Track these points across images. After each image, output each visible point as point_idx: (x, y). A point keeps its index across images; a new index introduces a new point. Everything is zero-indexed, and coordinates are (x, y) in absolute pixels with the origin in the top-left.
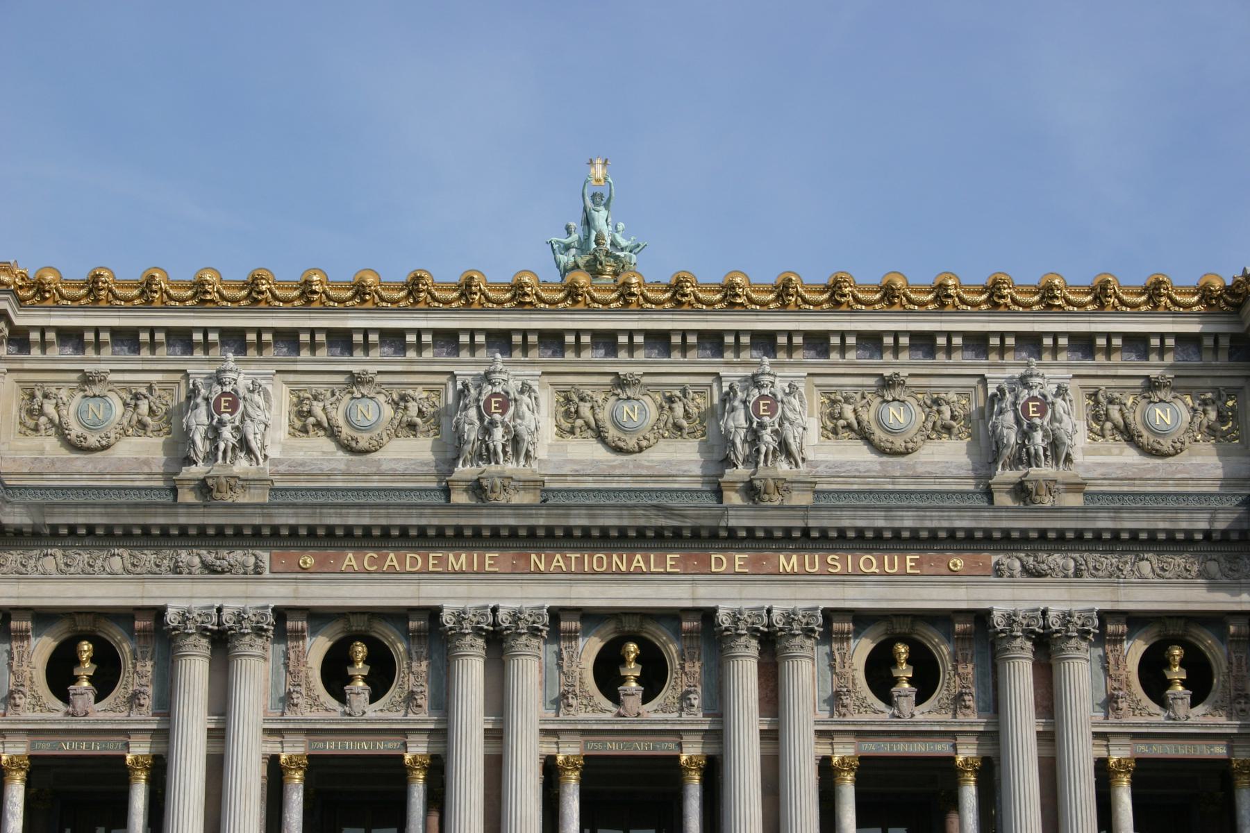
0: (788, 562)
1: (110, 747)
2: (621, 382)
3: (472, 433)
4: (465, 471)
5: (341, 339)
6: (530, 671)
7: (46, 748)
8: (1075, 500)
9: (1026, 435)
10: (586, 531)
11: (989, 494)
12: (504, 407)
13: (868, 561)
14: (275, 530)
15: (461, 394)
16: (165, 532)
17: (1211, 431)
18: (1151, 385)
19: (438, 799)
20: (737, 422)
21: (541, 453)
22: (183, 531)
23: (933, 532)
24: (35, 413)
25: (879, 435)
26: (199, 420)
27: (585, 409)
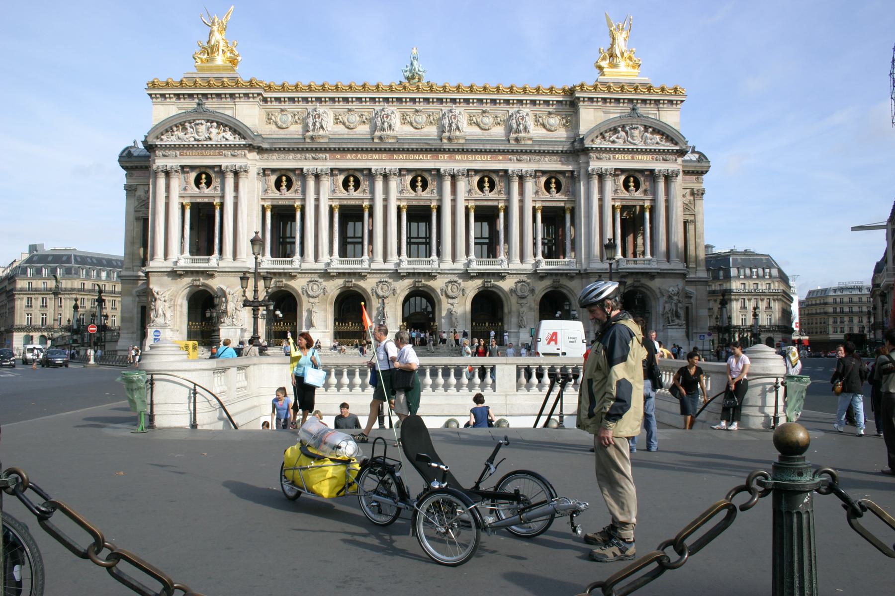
0: (458, 157)
1: (291, 203)
2: (417, 111)
3: (379, 124)
4: (377, 133)
5: (346, 100)
6: (394, 184)
7: (275, 203)
8: (530, 142)
9: (518, 125)
10: (408, 150)
11: (509, 140)
12: (387, 117)
13: (478, 157)
14: (330, 149)
15: (376, 114)
16: (303, 149)
17: (564, 125)
18: (550, 113)
19: (371, 215)
20: (446, 122)
21: (397, 129)
22: (307, 149)
23: (495, 151)
24: (269, 119)
25: (482, 125)
26: (310, 121)
27: (408, 118)
